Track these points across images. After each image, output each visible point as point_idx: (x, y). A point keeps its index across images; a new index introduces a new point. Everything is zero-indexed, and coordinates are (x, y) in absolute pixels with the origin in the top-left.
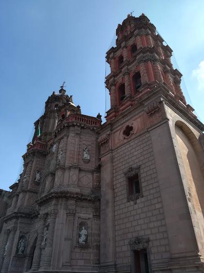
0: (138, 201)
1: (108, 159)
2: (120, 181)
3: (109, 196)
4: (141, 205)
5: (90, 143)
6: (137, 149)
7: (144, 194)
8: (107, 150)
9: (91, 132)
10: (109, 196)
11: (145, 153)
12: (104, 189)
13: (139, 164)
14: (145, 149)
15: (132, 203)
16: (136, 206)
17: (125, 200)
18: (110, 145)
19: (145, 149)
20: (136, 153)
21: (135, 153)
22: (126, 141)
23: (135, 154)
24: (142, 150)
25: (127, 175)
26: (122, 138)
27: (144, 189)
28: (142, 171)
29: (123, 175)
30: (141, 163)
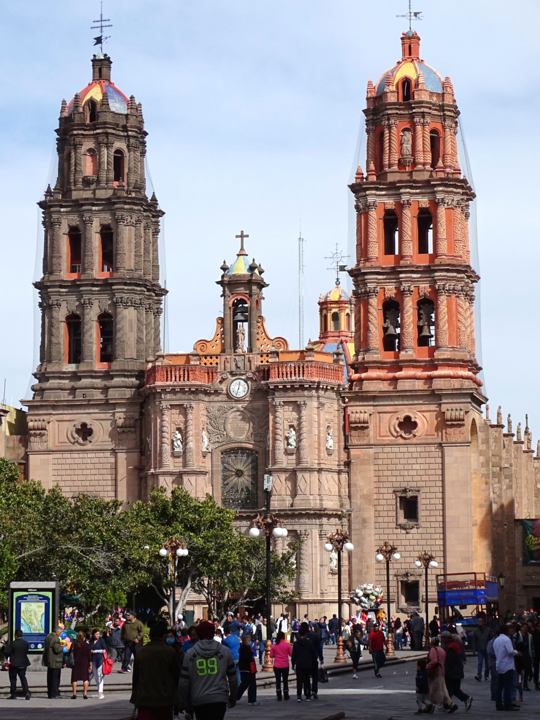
0: (414, 531)
1: (366, 458)
2: (386, 496)
3: (370, 513)
4: (416, 537)
5: (331, 417)
6: (419, 461)
7: (423, 525)
8: (365, 442)
9: (333, 395)
10: (370, 513)
11: (430, 472)
12: (359, 502)
13: (420, 484)
14: (432, 466)
15: (403, 531)
16: (409, 536)
17: (394, 525)
18: (371, 433)
19: (432, 466)
20: (417, 467)
21: (417, 467)
22: (401, 441)
23: (415, 467)
24: (427, 467)
25: (399, 494)
26: (395, 434)
27: (423, 519)
28: (423, 496)
29: (391, 490)
30: (423, 484)
